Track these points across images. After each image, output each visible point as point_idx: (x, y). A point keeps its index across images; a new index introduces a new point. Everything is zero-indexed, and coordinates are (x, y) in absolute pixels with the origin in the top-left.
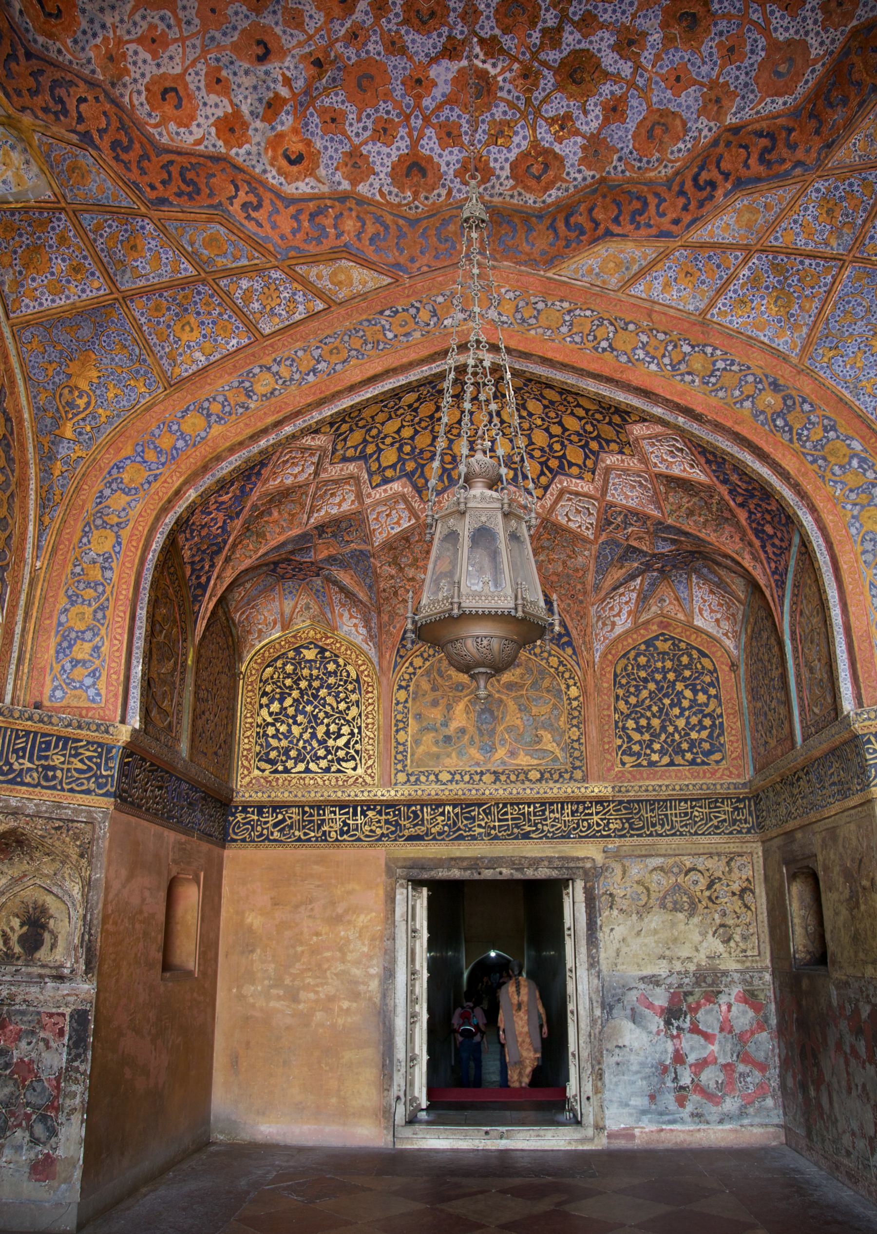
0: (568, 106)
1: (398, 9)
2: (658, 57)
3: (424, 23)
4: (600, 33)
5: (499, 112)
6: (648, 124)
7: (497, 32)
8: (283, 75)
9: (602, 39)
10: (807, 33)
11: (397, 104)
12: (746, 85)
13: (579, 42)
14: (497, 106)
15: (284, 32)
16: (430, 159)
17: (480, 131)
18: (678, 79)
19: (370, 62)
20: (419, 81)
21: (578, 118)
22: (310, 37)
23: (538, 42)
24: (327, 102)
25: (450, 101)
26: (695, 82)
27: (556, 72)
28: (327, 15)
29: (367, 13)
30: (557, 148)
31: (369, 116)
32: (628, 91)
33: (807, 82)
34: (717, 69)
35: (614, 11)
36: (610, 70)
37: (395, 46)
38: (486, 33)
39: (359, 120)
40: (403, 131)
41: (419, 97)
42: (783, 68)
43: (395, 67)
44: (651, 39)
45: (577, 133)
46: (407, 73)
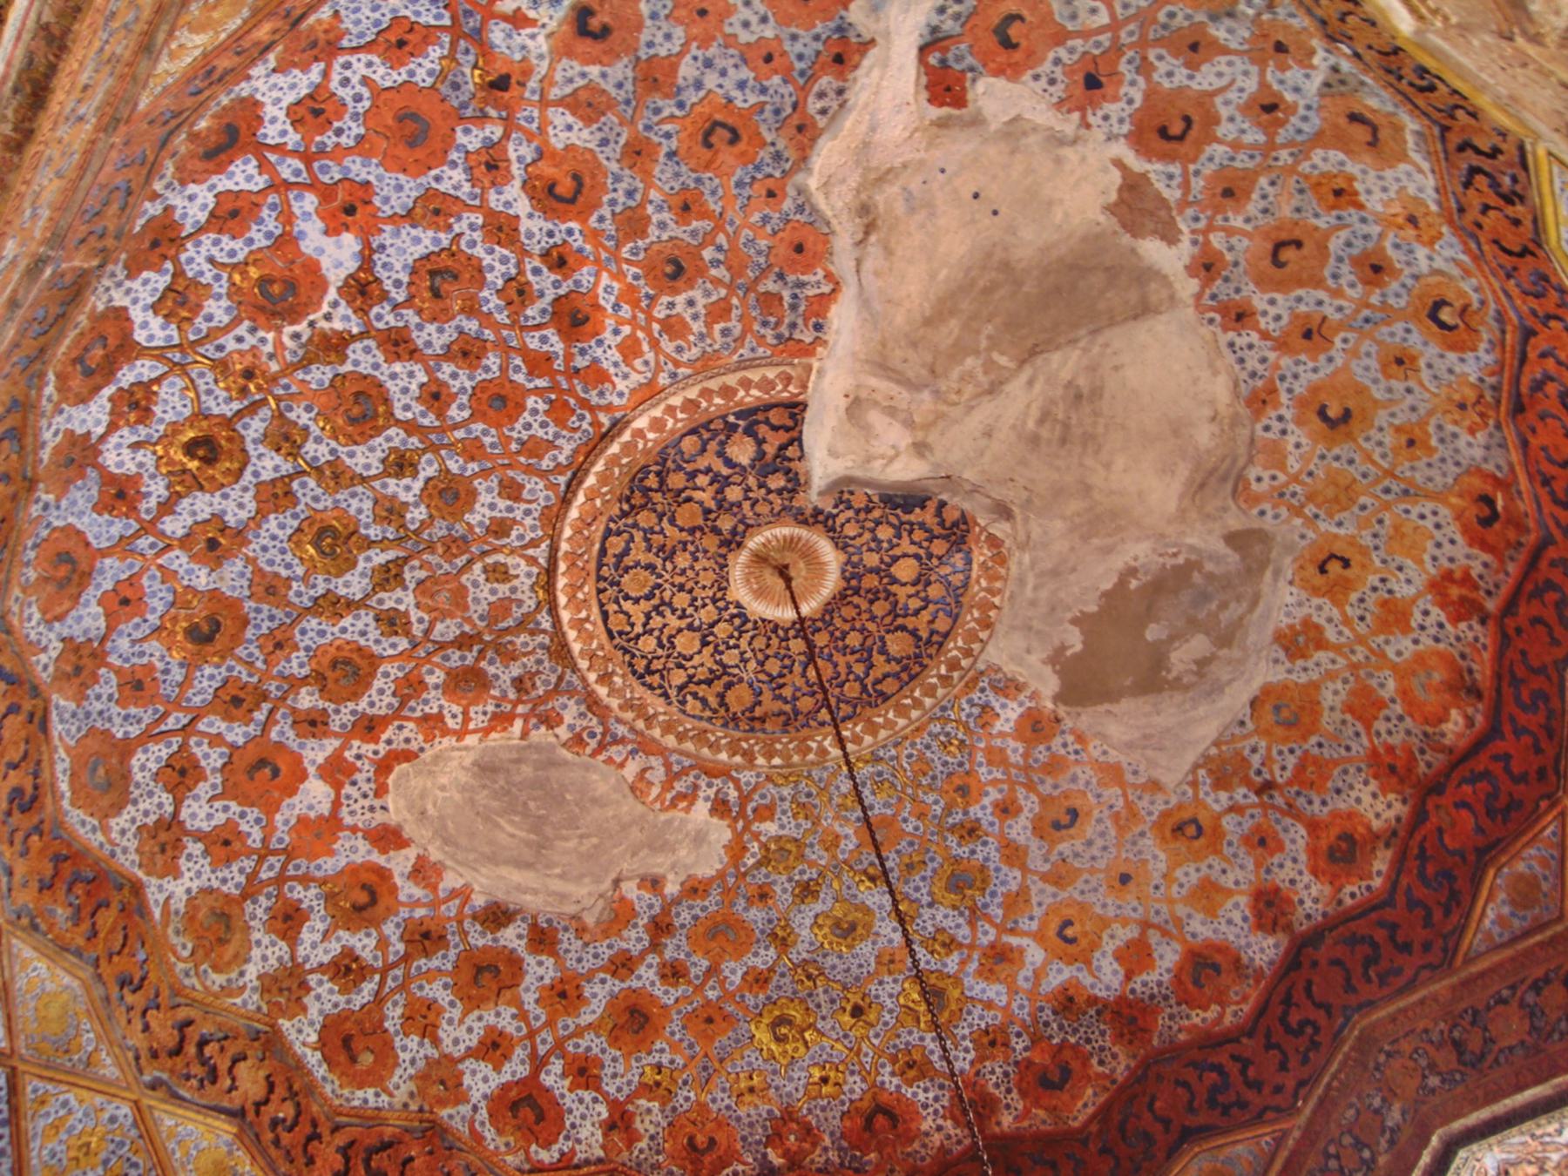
0: (162, 420)
1: (479, 251)
2: (168, 575)
3: (433, 273)
4: (252, 506)
5: (218, 309)
6: (79, 553)
7: (347, 367)
8: (532, 23)
9: (241, 506)
10: (135, 802)
11: (340, 153)
12: (88, 715)
13: (256, 474)
14: (228, 310)
15: (583, 75)
16: (221, 169)
17: (206, 267)
18: (125, 602)
19: (440, 157)
20: (350, 210)
21: (134, 432)
22: (544, 103)
23: (292, 416)
24: (435, 52)
25: (286, 241)
26: (110, 628)
27: (228, 423)
28: (554, 154)
29: (508, 204)
30: (108, 391)
31: (358, 98)
32: (139, 520)
33: (83, 823)
34: (118, 662)
35: (274, 538)
36: (185, 503)
37: (435, 209)
38: (356, 351)
39: (365, 81)
40: (293, 138)
41: (326, 193)
42: (101, 771)
43: (399, 188)
44: (204, 571)
45: (112, 427)
46: (377, 201)
